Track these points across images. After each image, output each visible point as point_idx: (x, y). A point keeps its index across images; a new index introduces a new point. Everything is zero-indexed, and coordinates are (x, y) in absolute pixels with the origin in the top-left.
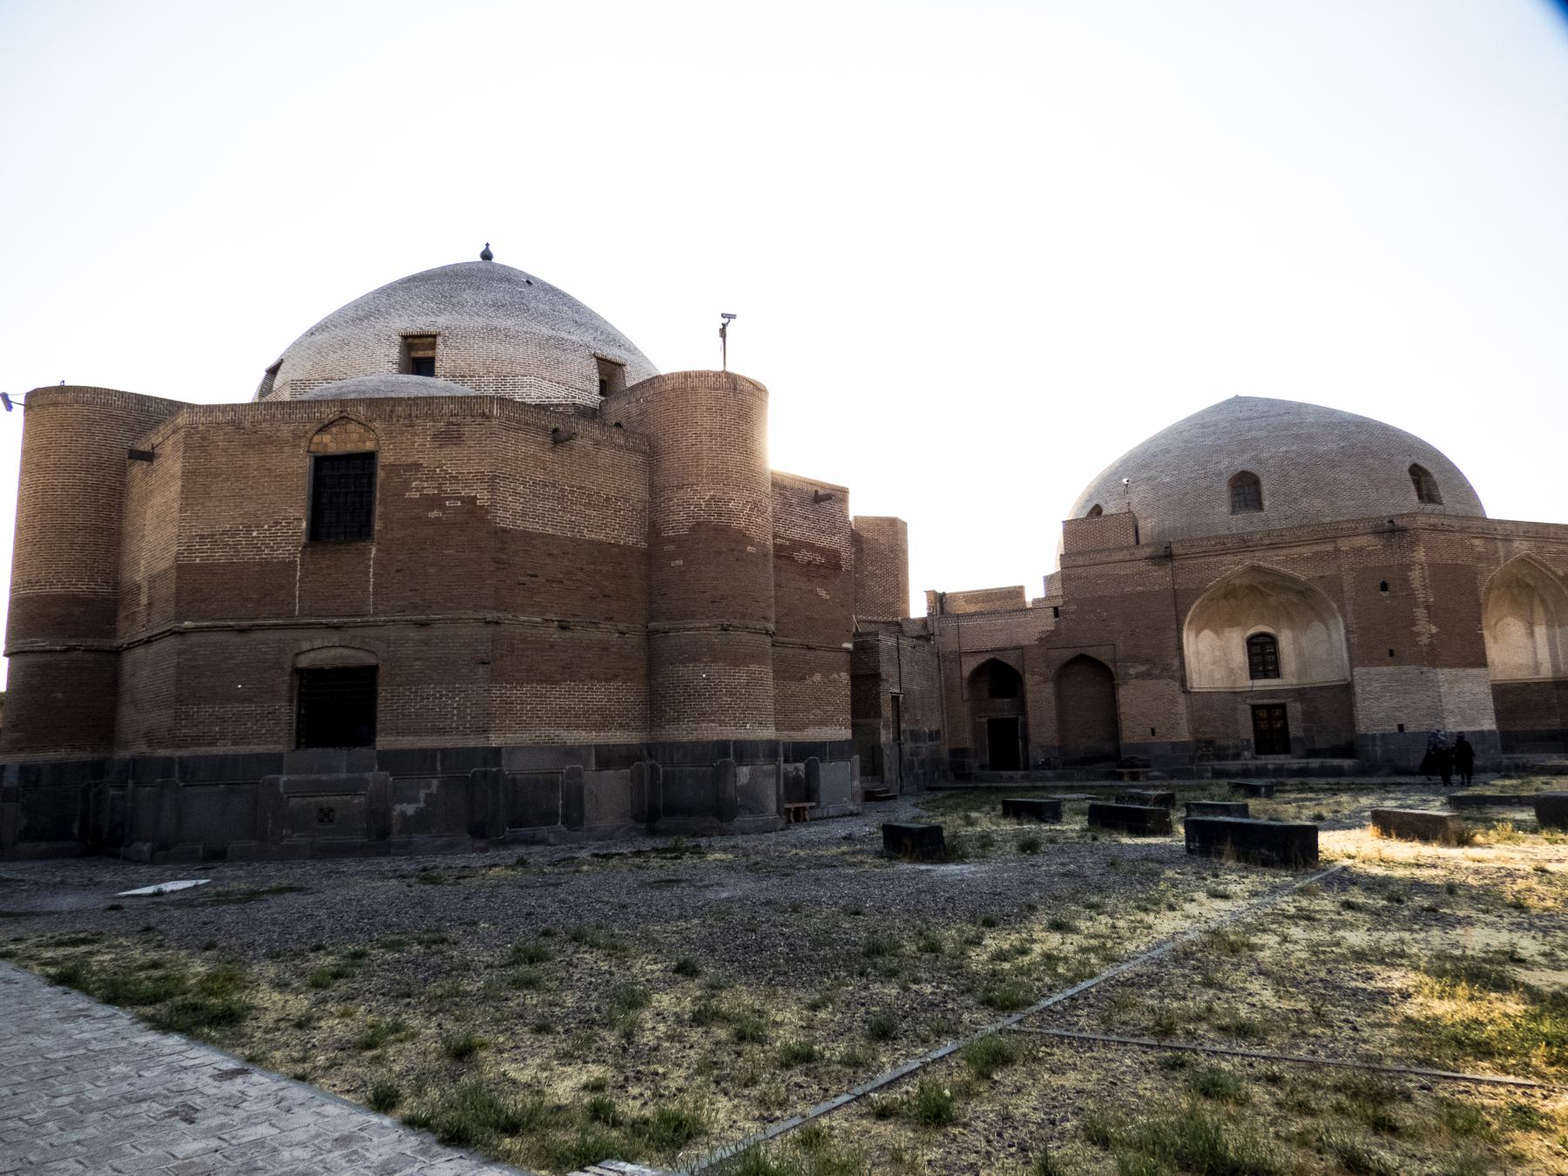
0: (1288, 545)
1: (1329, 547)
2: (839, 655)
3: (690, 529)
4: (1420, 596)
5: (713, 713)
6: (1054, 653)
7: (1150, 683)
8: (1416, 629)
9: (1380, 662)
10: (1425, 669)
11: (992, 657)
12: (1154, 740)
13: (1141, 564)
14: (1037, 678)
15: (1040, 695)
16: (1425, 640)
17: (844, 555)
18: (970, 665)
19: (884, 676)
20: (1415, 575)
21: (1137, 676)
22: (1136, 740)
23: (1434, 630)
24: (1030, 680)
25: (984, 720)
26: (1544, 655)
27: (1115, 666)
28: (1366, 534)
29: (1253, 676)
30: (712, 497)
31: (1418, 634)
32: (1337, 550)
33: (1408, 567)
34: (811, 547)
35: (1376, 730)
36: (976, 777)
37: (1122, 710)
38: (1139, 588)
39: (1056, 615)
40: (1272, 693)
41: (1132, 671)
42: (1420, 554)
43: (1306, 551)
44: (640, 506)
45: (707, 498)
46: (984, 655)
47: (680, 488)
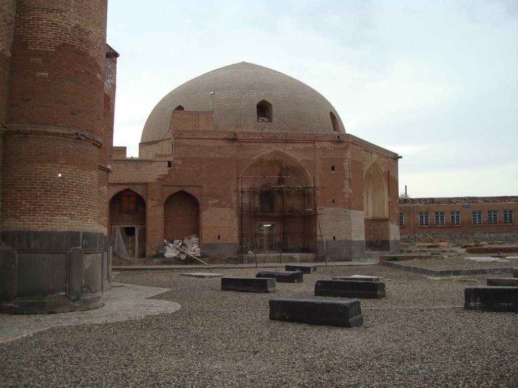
0: (294, 142)
1: (311, 145)
3: (57, 48)
4: (347, 173)
5: (66, 208)
8: (344, 190)
10: (345, 210)
11: (127, 187)
13: (220, 142)
14: (155, 203)
16: (347, 196)
20: (346, 164)
21: (213, 205)
24: (150, 204)
27: (201, 199)
28: (328, 141)
30: (77, 26)
31: (344, 193)
32: (314, 147)
33: (343, 160)
35: (325, 239)
39: (169, 166)
41: (210, 202)
42: (348, 155)
43: (301, 146)
44: (9, 18)
45: (73, 25)
46: (123, 186)
47: (49, 11)
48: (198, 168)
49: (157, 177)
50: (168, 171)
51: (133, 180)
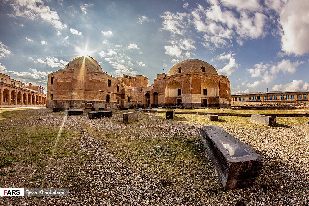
1: (181, 77)
7: (161, 96)
9: (186, 93)
15: (151, 97)
16: (190, 90)
18: (145, 93)
20: (190, 81)
21: (161, 95)
22: (160, 103)
23: (192, 88)
26: (215, 93)
29: (178, 95)
33: (190, 80)
34: (96, 80)
40: (180, 97)
42: (191, 78)
43: (179, 77)
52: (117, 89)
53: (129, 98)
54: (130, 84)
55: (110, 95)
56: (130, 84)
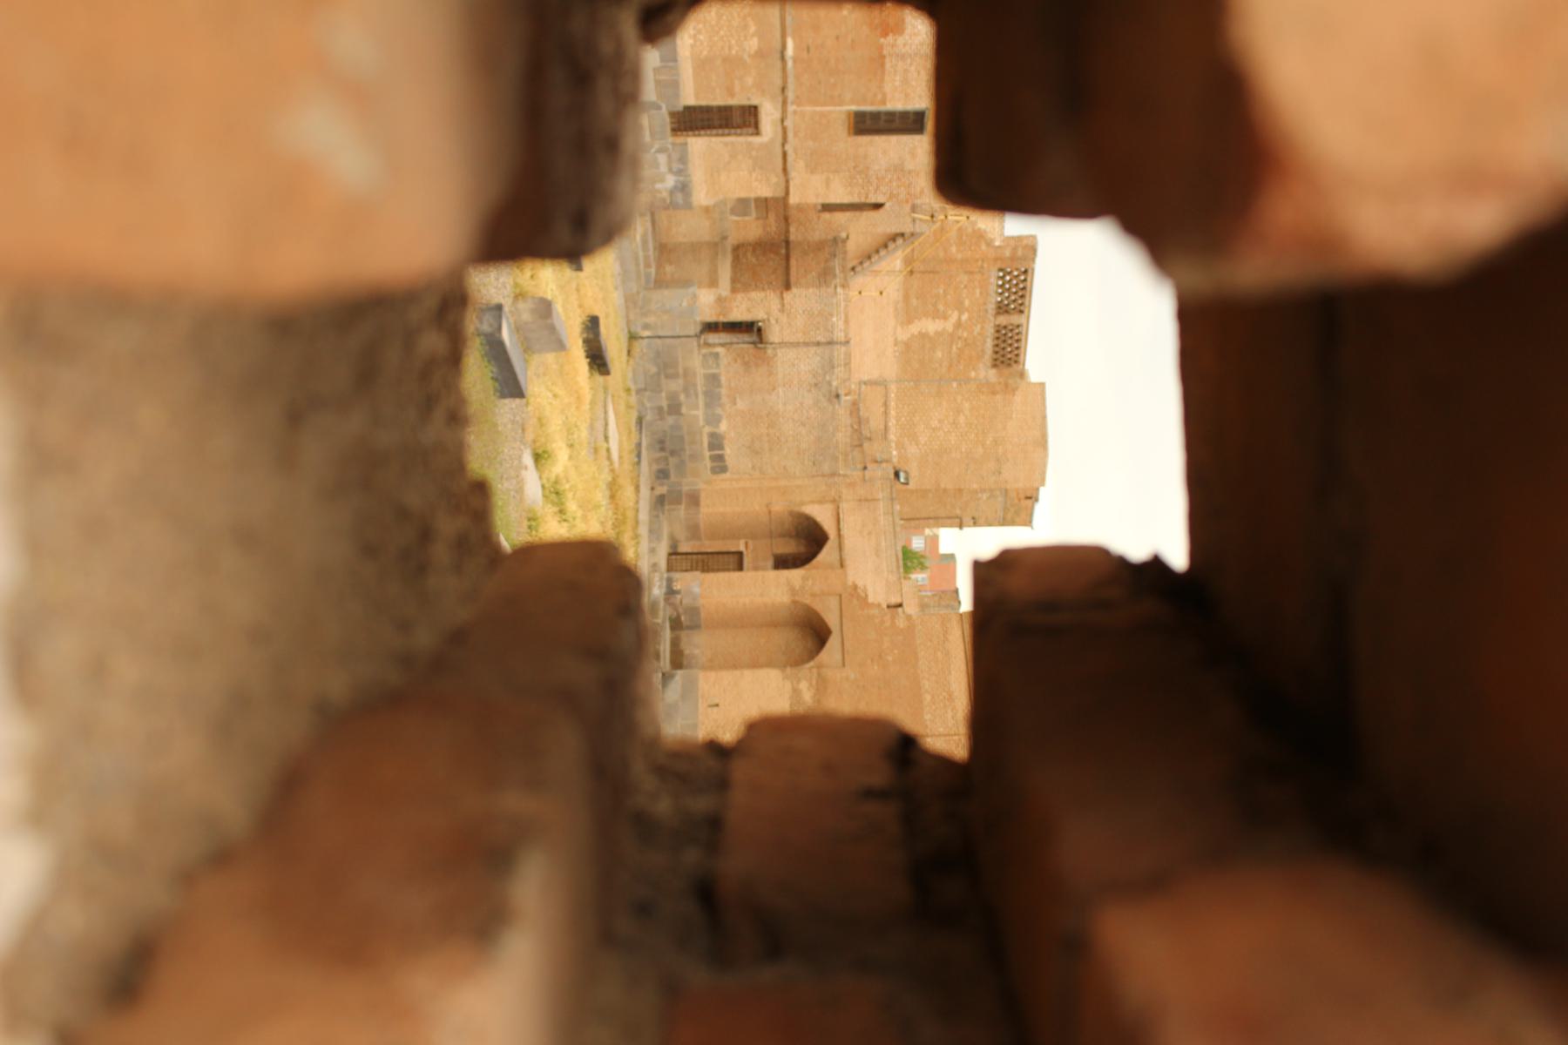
2: (778, 34)
6: (833, 603)
12: (702, 706)
17: (900, 41)
19: (788, 296)
24: (795, 575)
25: (742, 548)
36: (657, 516)
37: (748, 673)
38: (928, 697)
41: (803, 686)
48: (890, 658)
49: (860, 583)
50: (876, 602)
51: (847, 543)
52: (839, 195)
53: (748, 328)
54: (931, 326)
55: (757, 133)
56: (931, 326)
